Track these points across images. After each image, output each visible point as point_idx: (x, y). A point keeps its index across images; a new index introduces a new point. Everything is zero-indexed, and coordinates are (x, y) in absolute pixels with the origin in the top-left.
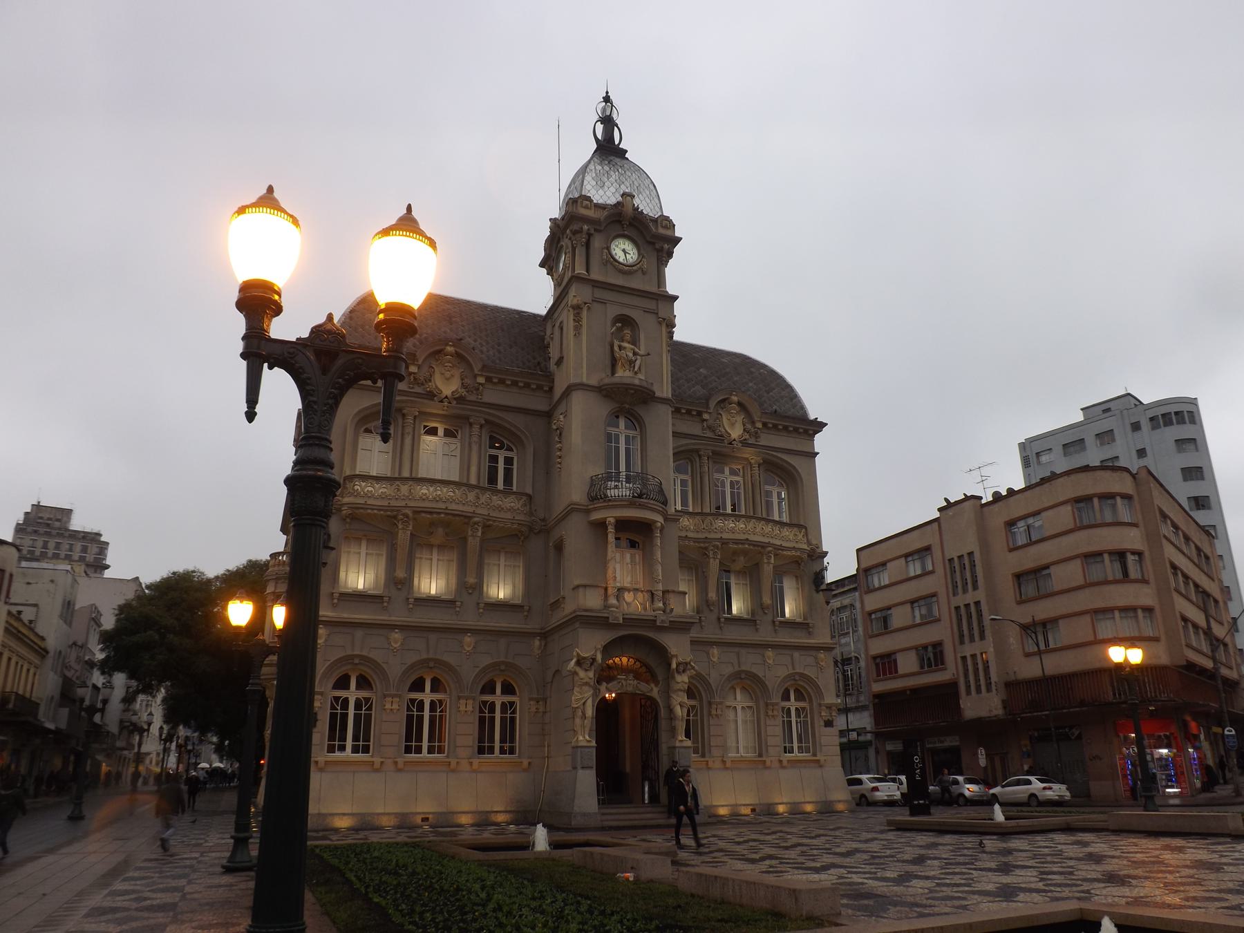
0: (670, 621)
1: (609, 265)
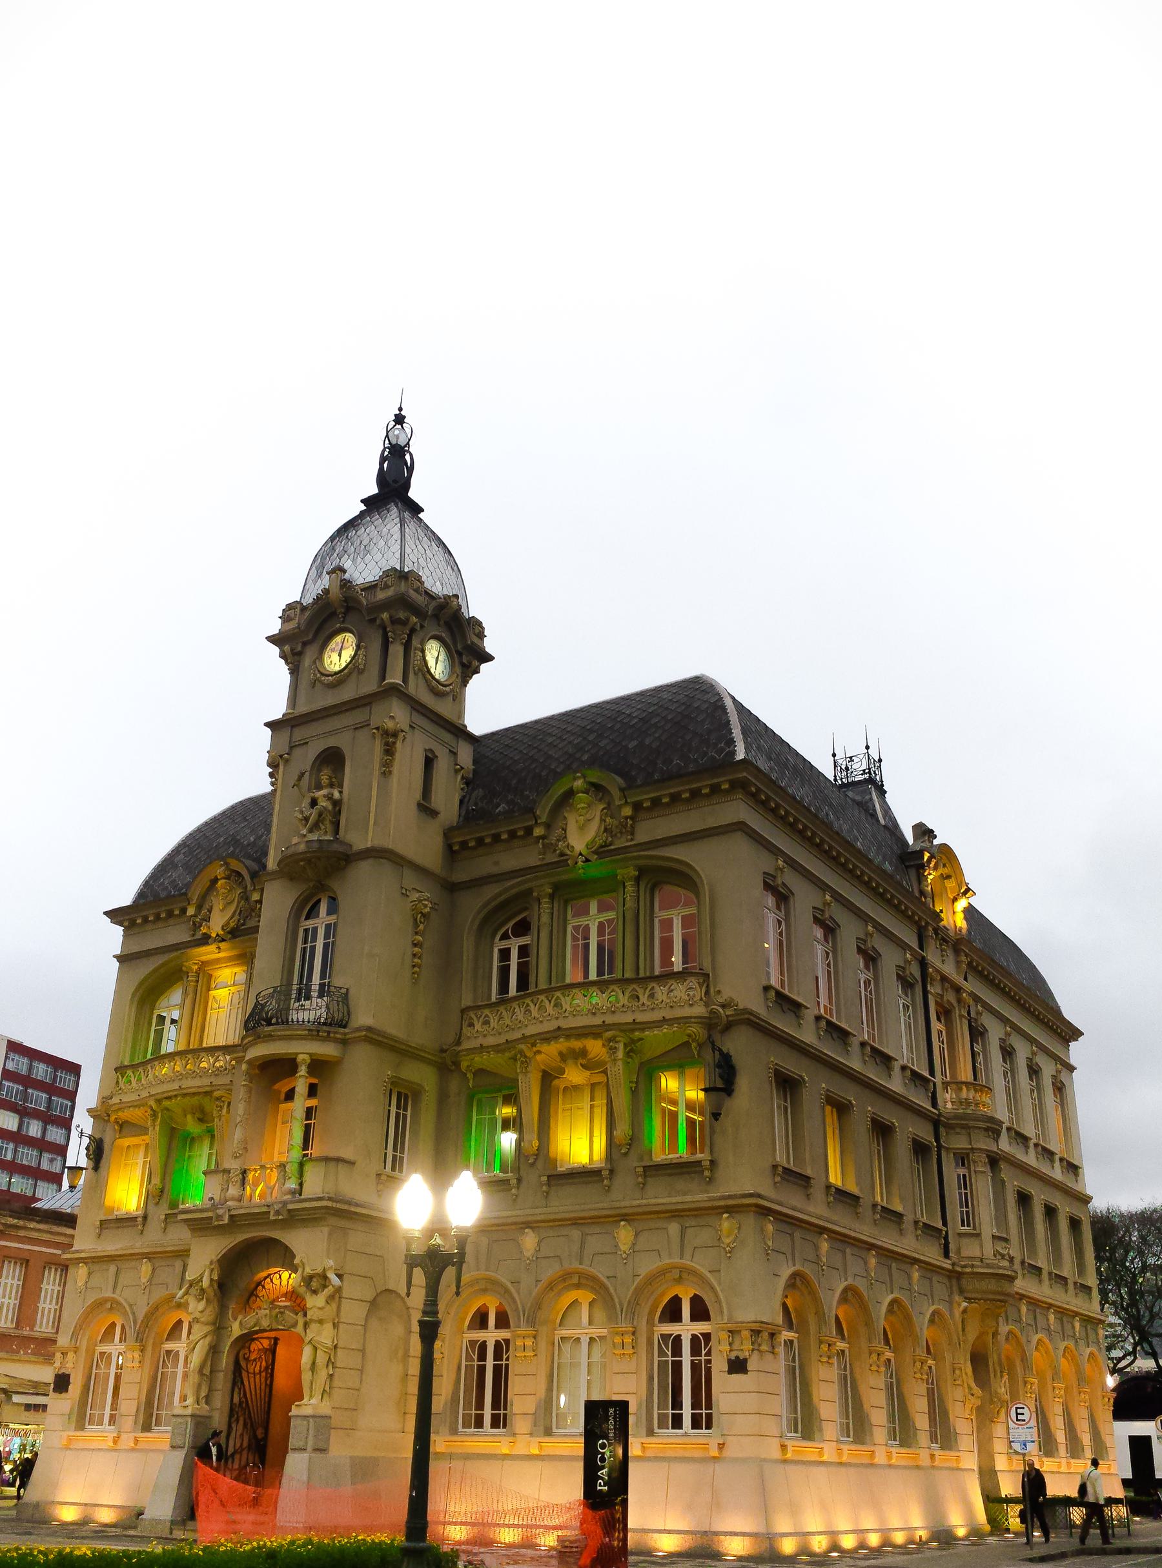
0: (289, 1211)
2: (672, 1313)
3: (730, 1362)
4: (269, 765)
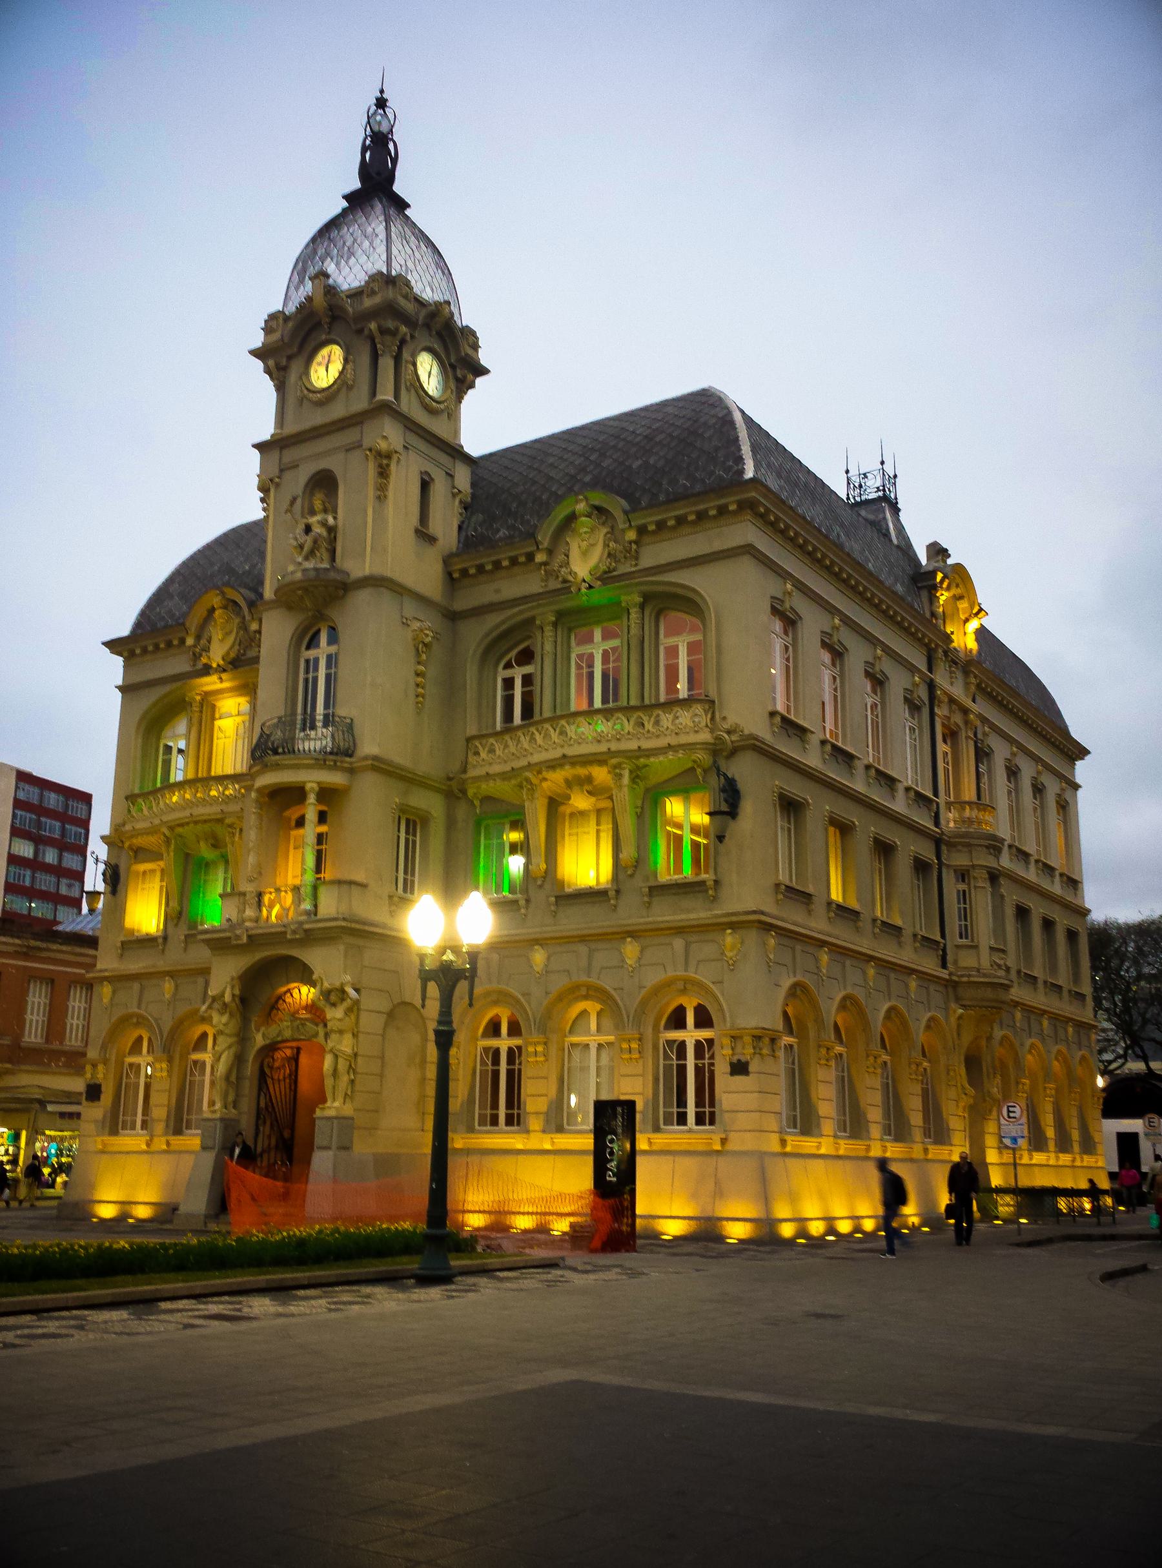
0: (306, 931)
2: (677, 1020)
3: (732, 1065)
4: (261, 489)
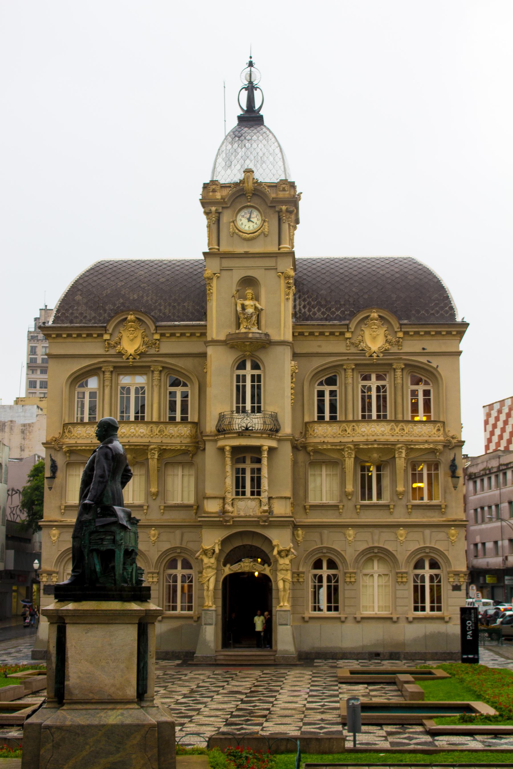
0: (270, 521)
1: (235, 236)
2: (419, 565)
